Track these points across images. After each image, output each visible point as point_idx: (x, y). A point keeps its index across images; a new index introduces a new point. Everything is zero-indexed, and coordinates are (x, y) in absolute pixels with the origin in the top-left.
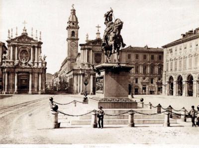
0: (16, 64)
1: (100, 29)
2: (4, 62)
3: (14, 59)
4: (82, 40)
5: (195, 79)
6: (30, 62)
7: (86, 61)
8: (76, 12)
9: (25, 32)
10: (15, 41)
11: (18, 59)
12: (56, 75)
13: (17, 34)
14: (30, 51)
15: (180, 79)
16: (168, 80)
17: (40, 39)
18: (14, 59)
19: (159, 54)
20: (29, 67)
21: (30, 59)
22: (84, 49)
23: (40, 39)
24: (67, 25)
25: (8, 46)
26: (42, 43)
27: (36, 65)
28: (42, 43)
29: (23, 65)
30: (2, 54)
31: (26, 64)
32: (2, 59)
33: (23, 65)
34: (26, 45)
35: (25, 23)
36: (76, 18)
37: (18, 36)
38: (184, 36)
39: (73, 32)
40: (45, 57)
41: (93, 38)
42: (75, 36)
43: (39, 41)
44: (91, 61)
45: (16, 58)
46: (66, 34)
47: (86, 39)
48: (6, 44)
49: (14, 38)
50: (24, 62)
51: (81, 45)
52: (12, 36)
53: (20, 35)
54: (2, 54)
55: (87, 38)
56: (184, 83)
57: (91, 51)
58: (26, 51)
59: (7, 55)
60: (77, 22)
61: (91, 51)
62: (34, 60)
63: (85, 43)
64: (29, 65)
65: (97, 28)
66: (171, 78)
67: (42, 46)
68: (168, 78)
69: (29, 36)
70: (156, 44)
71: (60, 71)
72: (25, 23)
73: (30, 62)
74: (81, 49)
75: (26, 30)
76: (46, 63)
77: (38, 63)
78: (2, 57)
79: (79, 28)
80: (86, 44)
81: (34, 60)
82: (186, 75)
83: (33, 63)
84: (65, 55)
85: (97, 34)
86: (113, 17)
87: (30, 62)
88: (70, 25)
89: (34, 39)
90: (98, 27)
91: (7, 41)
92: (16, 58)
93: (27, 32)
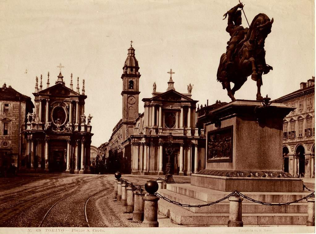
0: (46, 128)
2: (29, 125)
3: (43, 119)
4: (146, 91)
9: (60, 80)
12: (104, 146)
13: (48, 84)
14: (68, 109)
17: (83, 90)
18: (43, 119)
20: (66, 132)
21: (68, 120)
22: (149, 106)
23: (83, 90)
24: (122, 72)
25: (36, 101)
26: (86, 97)
28: (86, 97)
30: (27, 114)
31: (62, 127)
32: (26, 121)
34: (60, 98)
35: (61, 66)
37: (50, 86)
38: (303, 84)
40: (91, 118)
41: (163, 89)
42: (135, 87)
43: (81, 94)
44: (160, 125)
46: (119, 85)
47: (152, 91)
48: (33, 98)
49: (45, 87)
51: (144, 100)
52: (41, 86)
53: (52, 84)
54: (27, 114)
55: (155, 89)
60: (137, 68)
62: (73, 121)
63: (151, 96)
64: (66, 129)
65: (169, 75)
67: (85, 100)
69: (68, 85)
71: (110, 140)
72: (61, 66)
73: (68, 125)
74: (145, 106)
76: (91, 127)
79: (139, 76)
81: (73, 121)
84: (118, 116)
85: (169, 83)
86: (243, 16)
88: (126, 72)
89: (75, 90)
90: (171, 73)
91: (35, 94)
93: (65, 80)
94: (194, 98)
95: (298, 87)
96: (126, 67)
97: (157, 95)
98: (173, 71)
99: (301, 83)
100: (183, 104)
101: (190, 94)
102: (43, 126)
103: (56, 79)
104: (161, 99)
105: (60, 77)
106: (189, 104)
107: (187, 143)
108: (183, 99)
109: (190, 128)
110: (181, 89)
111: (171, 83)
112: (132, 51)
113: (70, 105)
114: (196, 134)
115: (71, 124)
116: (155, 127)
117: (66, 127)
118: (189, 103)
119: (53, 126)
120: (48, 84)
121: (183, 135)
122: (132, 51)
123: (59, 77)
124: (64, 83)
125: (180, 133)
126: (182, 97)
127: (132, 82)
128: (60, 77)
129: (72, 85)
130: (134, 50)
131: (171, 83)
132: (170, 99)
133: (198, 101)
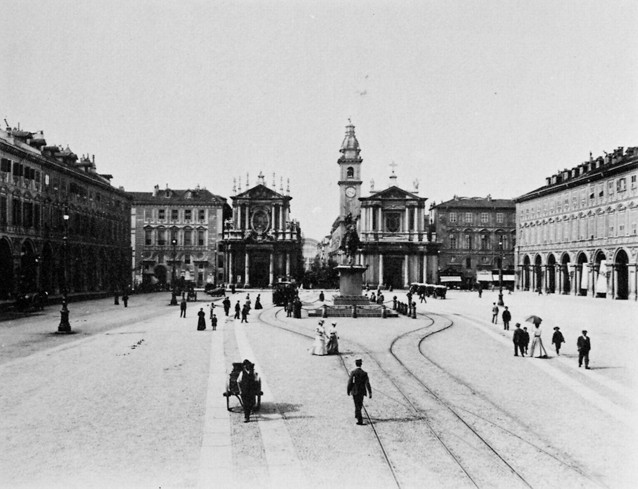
0: (246, 237)
1: (395, 169)
2: (227, 233)
3: (243, 227)
5: (632, 260)
6: (270, 233)
7: (370, 229)
8: (355, 130)
10: (244, 196)
11: (250, 228)
14: (270, 214)
15: (551, 259)
16: (522, 263)
17: (288, 191)
18: (243, 227)
19: (508, 208)
21: (270, 227)
22: (367, 207)
24: (340, 155)
25: (234, 205)
27: (281, 237)
29: (259, 238)
30: (224, 221)
31: (264, 235)
32: (224, 228)
33: (259, 238)
34: (261, 201)
36: (356, 144)
37: (250, 187)
39: (351, 169)
41: (382, 187)
42: (355, 175)
44: (380, 229)
45: (247, 227)
46: (337, 173)
48: (230, 202)
49: (243, 191)
50: (260, 233)
53: (253, 185)
55: (372, 186)
56: (543, 269)
57: (380, 209)
58: (263, 213)
59: (232, 221)
60: (358, 152)
61: (380, 209)
62: (277, 227)
63: (369, 195)
64: (269, 237)
65: (391, 168)
66: (527, 259)
67: (291, 202)
68: (522, 258)
69: (269, 186)
70: (505, 193)
73: (270, 232)
75: (263, 177)
77: (284, 234)
78: (223, 224)
79: (361, 161)
80: (371, 198)
81: (277, 227)
82: (547, 254)
83: (277, 234)
87: (270, 233)
89: (278, 191)
90: (393, 165)
92: (247, 227)
94: (421, 195)
95: (545, 183)
96: (343, 151)
97: (374, 194)
98: (396, 163)
99: (547, 179)
100: (408, 203)
101: (416, 190)
102: (242, 234)
104: (380, 197)
106: (415, 203)
107: (411, 249)
108: (408, 197)
109: (417, 232)
110: (405, 185)
113: (273, 208)
114: (425, 240)
115: (274, 231)
116: (373, 232)
117: (268, 235)
118: (415, 202)
119: (254, 234)
121: (407, 241)
123: (259, 177)
125: (405, 239)
126: (408, 195)
127: (351, 169)
130: (354, 127)
132: (392, 196)
133: (427, 199)
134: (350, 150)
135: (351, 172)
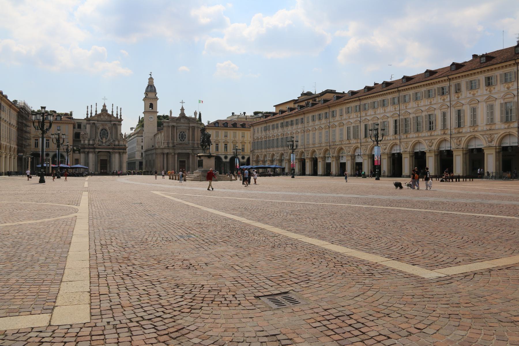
13: (96, 111)
17: (121, 116)
23: (121, 116)
35: (105, 99)
37: (98, 113)
41: (176, 114)
49: (93, 115)
52: (91, 113)
53: (99, 112)
69: (110, 112)
72: (105, 99)
89: (115, 115)
90: (182, 102)
96: (146, 93)
103: (102, 108)
105: (104, 106)
110: (189, 113)
111: (182, 109)
112: (151, 79)
120: (96, 111)
122: (151, 79)
124: (107, 111)
128: (104, 106)
129: (112, 112)
131: (182, 109)
134: (151, 91)
135: (151, 106)
